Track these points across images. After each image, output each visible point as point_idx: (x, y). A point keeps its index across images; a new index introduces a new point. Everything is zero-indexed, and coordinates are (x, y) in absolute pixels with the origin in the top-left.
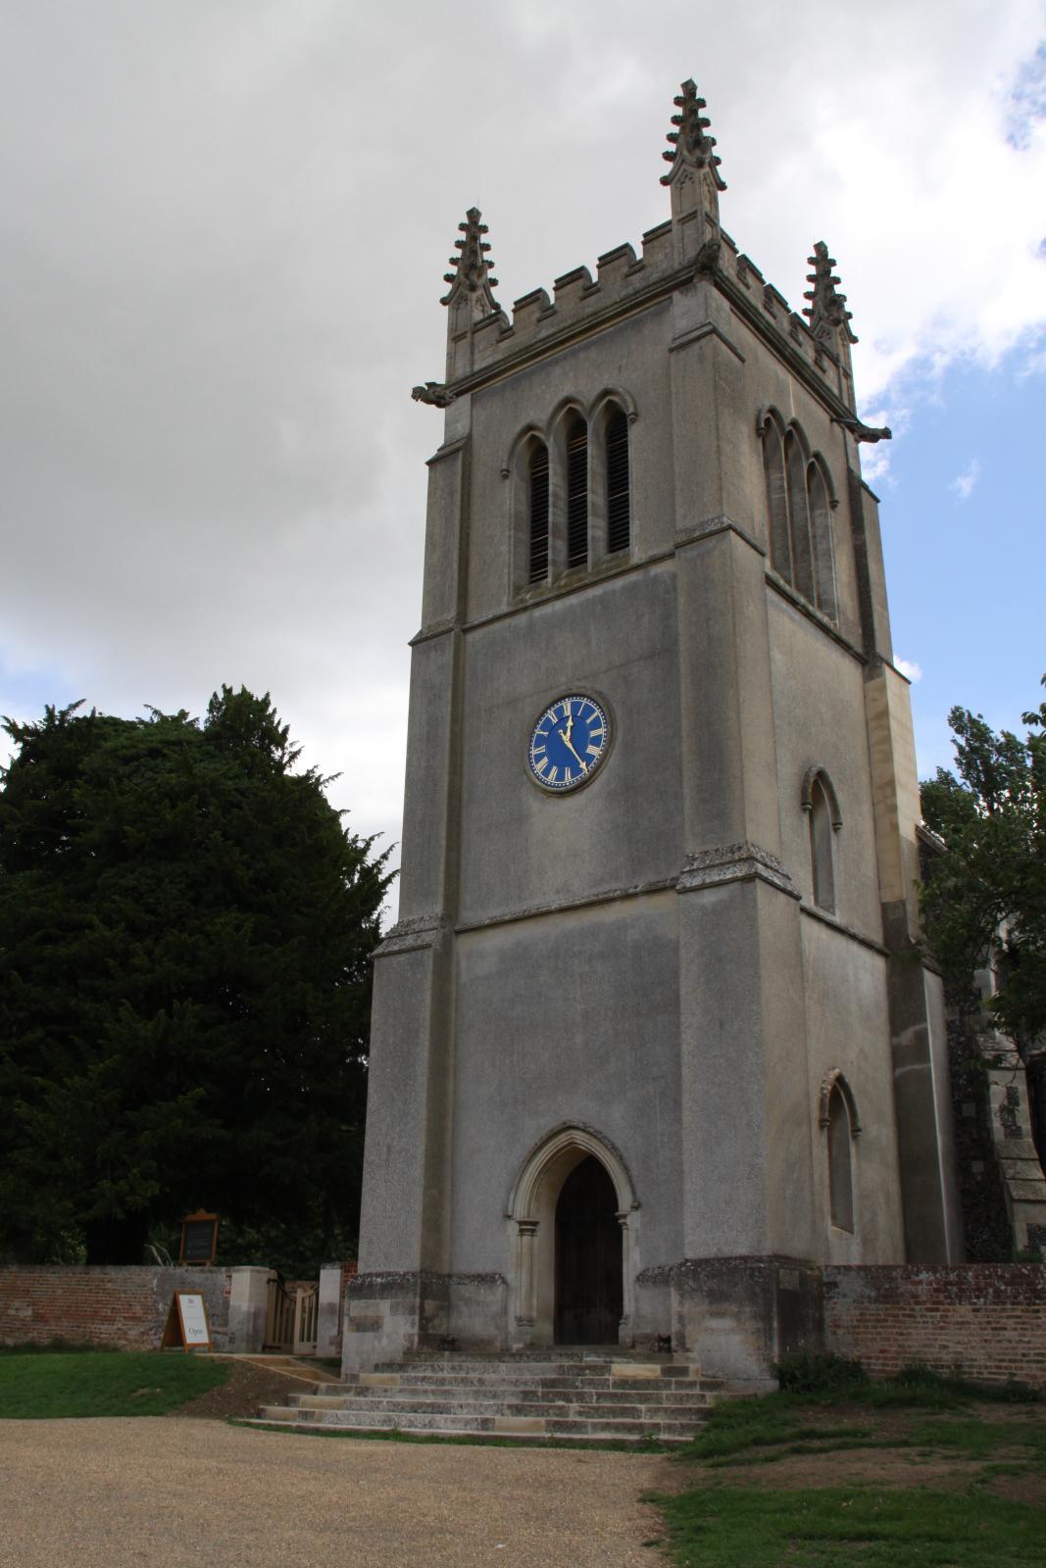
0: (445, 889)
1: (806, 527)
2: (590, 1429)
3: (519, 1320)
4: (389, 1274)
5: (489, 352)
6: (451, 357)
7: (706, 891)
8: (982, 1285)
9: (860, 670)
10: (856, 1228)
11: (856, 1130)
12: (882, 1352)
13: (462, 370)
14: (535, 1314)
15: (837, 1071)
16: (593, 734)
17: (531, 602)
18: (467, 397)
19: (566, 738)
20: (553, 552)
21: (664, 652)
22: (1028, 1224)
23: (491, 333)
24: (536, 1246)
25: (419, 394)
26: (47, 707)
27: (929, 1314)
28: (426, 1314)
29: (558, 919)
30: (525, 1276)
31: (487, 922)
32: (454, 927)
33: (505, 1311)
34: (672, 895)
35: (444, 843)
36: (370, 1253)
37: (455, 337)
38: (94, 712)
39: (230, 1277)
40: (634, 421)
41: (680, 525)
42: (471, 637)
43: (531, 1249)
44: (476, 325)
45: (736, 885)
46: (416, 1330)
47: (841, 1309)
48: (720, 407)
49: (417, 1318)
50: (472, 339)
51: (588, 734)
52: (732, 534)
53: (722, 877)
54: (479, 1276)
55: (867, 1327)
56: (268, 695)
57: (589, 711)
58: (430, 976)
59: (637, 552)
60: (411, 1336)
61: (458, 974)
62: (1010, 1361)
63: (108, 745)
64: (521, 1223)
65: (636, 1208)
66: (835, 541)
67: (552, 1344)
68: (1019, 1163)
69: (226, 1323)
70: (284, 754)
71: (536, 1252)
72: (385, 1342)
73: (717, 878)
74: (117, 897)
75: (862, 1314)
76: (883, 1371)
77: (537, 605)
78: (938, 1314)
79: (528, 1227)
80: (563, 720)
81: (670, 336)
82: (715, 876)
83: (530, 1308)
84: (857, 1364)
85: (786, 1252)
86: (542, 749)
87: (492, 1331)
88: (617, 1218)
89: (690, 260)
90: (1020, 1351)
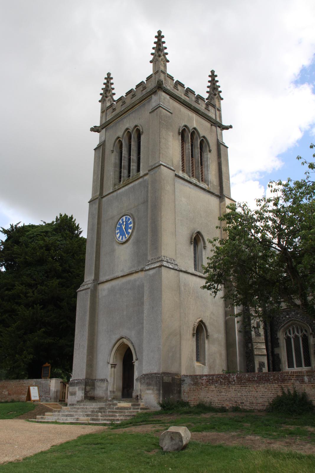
0: (95, 272)
1: (199, 159)
2: (101, 420)
3: (111, 391)
4: (79, 379)
5: (110, 116)
6: (101, 118)
7: (151, 270)
8: (217, 380)
9: (218, 200)
10: (206, 364)
11: (207, 336)
12: (194, 399)
13: (104, 122)
14: (115, 390)
15: (200, 319)
16: (130, 226)
17: (117, 188)
18: (104, 129)
19: (124, 227)
20: (123, 174)
21: (145, 202)
22: (259, 362)
23: (110, 110)
24: (116, 371)
25: (93, 130)
26: (10, 224)
27: (205, 388)
28: (87, 390)
29: (121, 279)
30: (112, 379)
31: (105, 281)
33: (107, 389)
34: (143, 273)
35: (94, 259)
36: (75, 374)
37: (102, 112)
38: (24, 224)
39: (50, 381)
40: (142, 134)
41: (150, 165)
42: (104, 199)
43: (114, 372)
44: (107, 108)
45: (157, 268)
46: (83, 395)
47: (185, 387)
48: (161, 129)
49: (84, 391)
50: (106, 112)
51: (129, 226)
52: (162, 166)
53: (154, 266)
54: (102, 379)
55: (191, 392)
56: (72, 215)
57: (129, 219)
58: (89, 296)
59: (142, 173)
60: (82, 396)
61: (99, 296)
62: (223, 401)
63: (27, 233)
64: (111, 365)
65: (137, 360)
66: (210, 162)
67: (121, 397)
68: (259, 344)
69: (49, 395)
70: (78, 232)
71: (116, 373)
72: (77, 398)
73: (153, 267)
74: (25, 277)
75: (190, 389)
76: (194, 404)
77: (118, 189)
78: (207, 388)
79: (114, 366)
80: (123, 222)
81: (151, 108)
82: (153, 266)
83: (114, 388)
84: (188, 403)
85: (169, 371)
86: (118, 231)
87: (104, 395)
88: (133, 363)
89: (158, 85)
90: (225, 398)
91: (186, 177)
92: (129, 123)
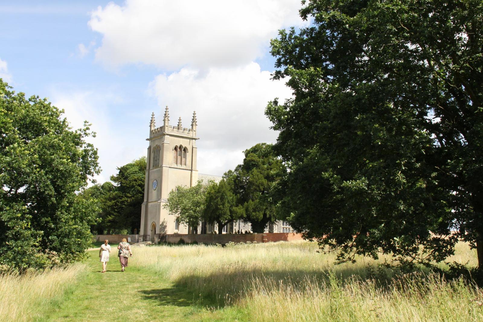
47: (167, 238)
79: (152, 231)
91: (175, 166)
92: (157, 143)
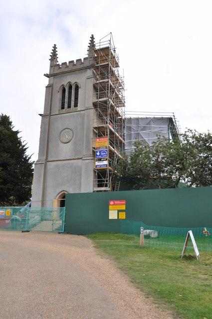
13: (52, 73)
23: (57, 67)
25: (45, 75)
29: (63, 161)
32: (47, 161)
34: (81, 160)
37: (51, 66)
59: (79, 108)
92: (72, 79)
